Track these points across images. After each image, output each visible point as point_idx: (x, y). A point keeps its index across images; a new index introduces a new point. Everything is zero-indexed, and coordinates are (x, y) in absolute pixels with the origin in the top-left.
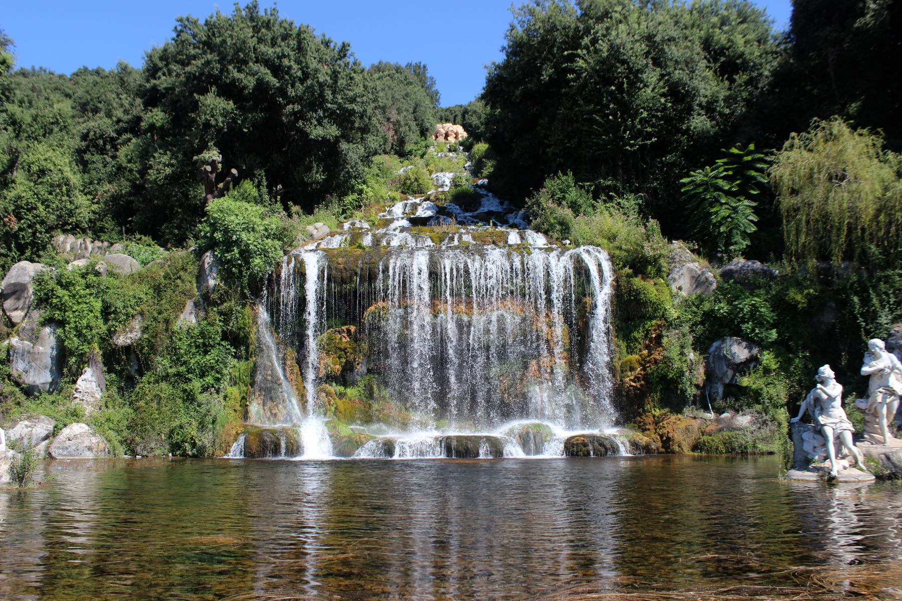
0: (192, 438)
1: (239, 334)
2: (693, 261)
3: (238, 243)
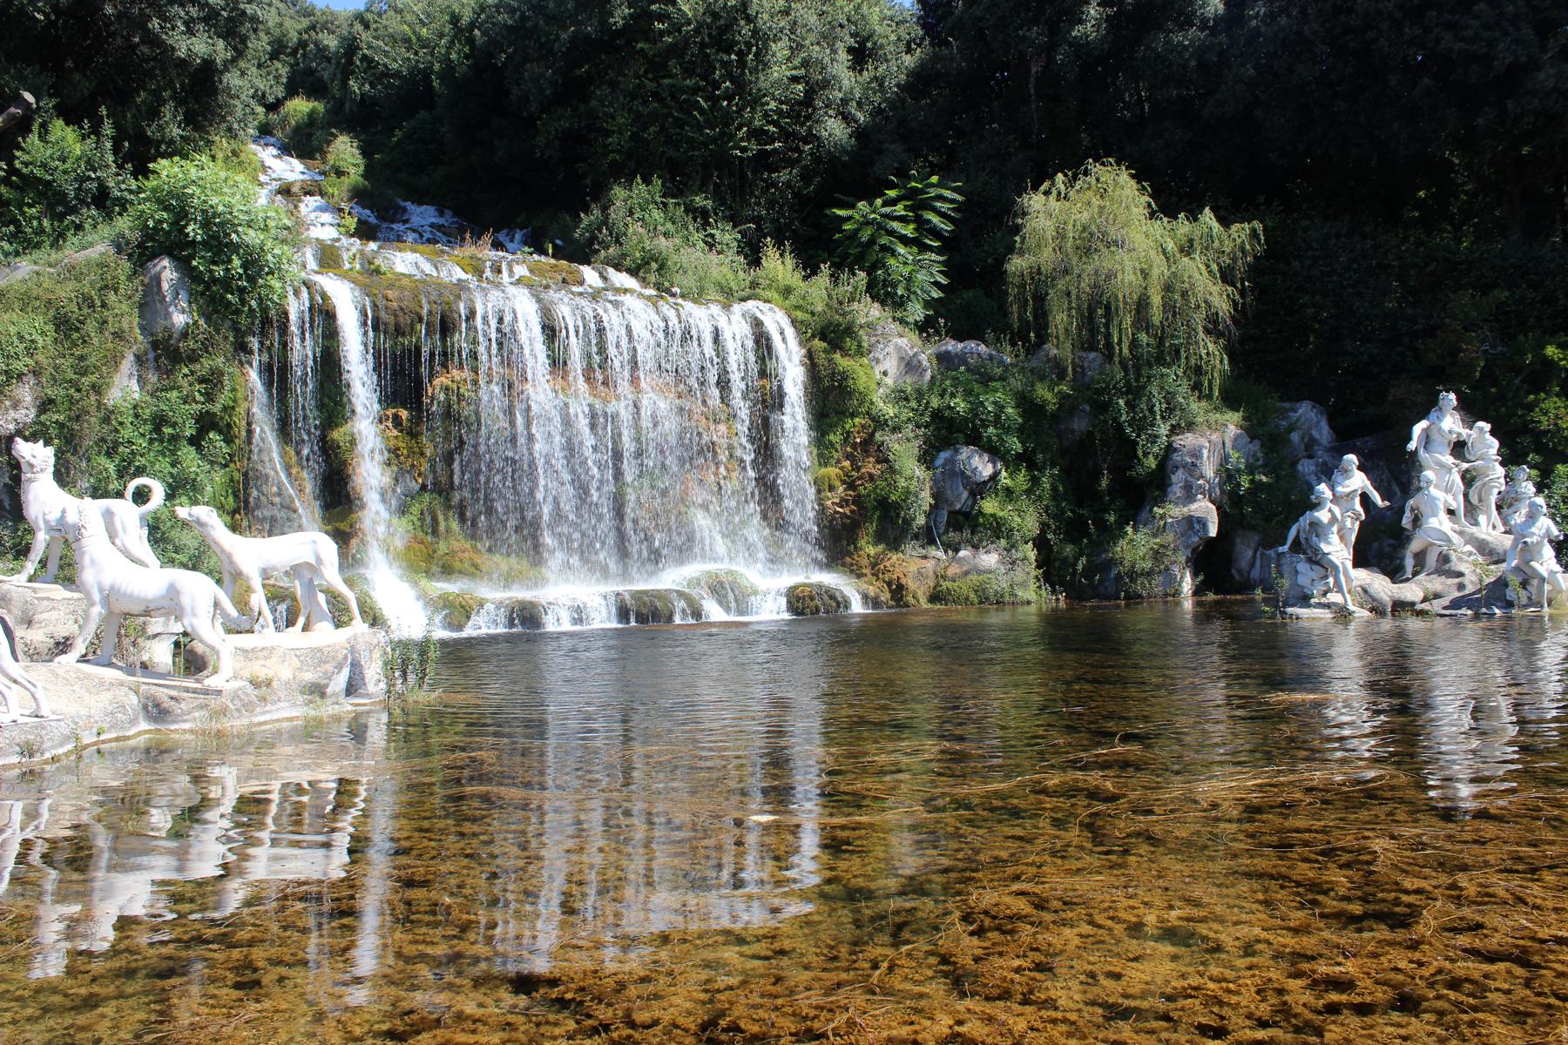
3: (235, 248)
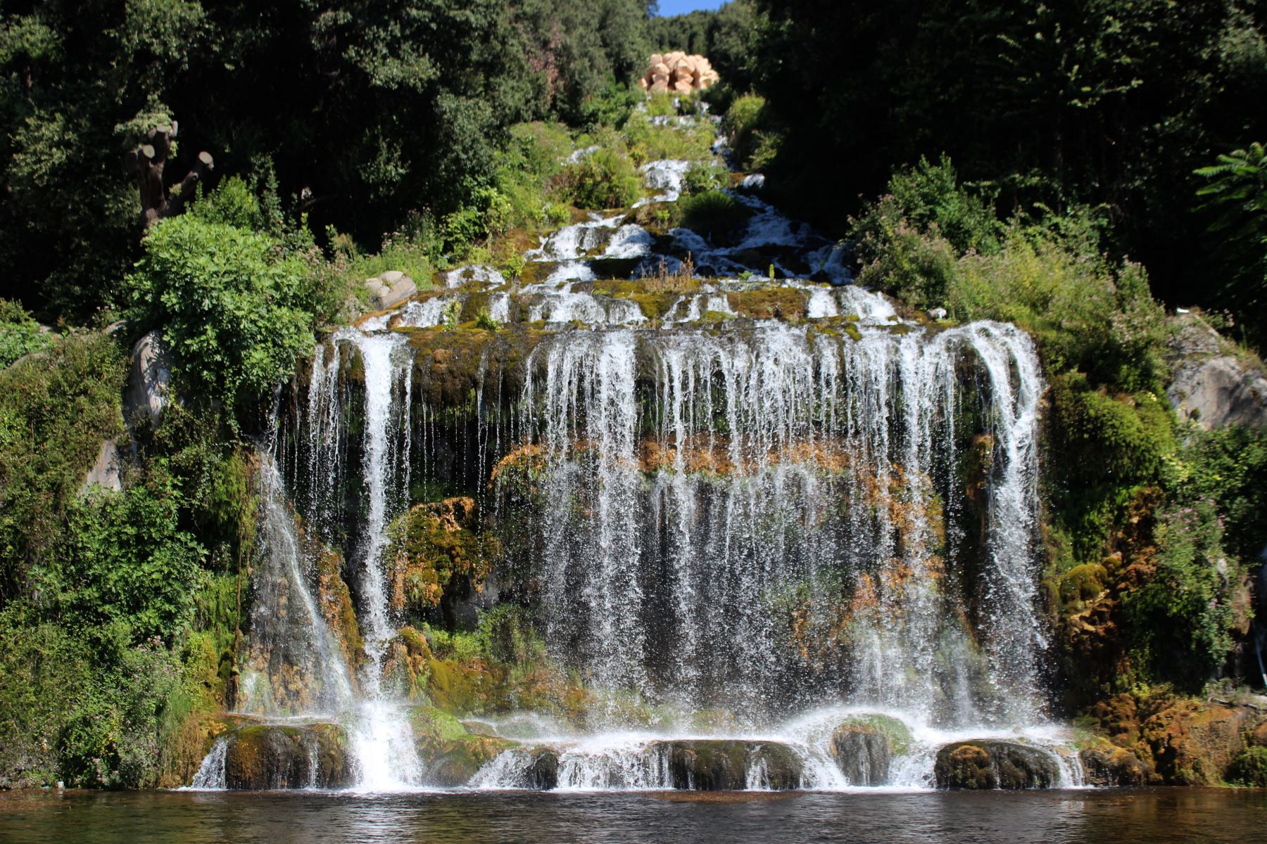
0: (109, 748)
1: (217, 515)
2: (1225, 354)
3: (214, 315)
